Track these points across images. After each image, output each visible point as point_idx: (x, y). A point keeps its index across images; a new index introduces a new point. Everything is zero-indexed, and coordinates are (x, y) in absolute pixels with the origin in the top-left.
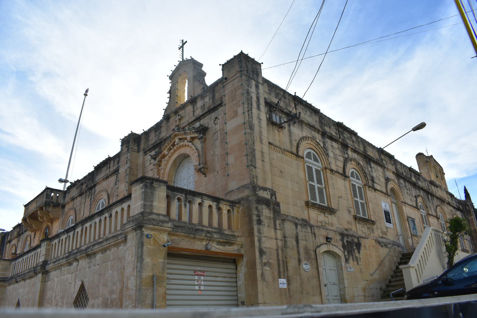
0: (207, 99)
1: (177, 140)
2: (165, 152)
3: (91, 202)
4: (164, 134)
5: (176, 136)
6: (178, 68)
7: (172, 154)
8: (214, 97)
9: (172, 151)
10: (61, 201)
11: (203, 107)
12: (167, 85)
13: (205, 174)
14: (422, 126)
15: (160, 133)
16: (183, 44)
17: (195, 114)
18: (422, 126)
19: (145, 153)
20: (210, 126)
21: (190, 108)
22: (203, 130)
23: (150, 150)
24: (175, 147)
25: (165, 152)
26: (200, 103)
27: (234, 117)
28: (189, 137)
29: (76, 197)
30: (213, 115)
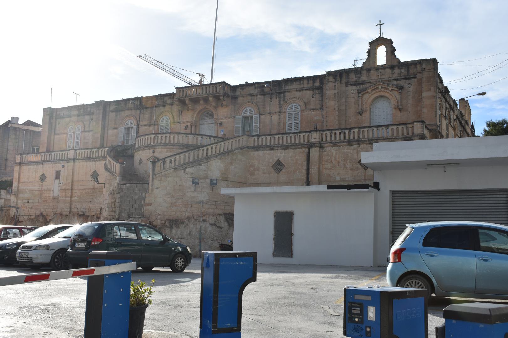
0: (403, 71)
1: (380, 87)
2: (369, 91)
3: (280, 104)
4: (364, 78)
5: (380, 84)
6: (377, 40)
7: (374, 93)
8: (408, 71)
9: (374, 92)
10: (231, 94)
11: (400, 74)
12: (368, 47)
13: (401, 111)
14: (484, 94)
15: (361, 77)
16: (380, 25)
17: (394, 76)
18: (484, 94)
19: (347, 85)
20: (405, 87)
21: (388, 71)
22: (401, 88)
23: (351, 85)
24: (377, 90)
25: (369, 91)
26: (397, 71)
27: (428, 91)
28: (390, 89)
29: (257, 95)
30: (408, 82)
